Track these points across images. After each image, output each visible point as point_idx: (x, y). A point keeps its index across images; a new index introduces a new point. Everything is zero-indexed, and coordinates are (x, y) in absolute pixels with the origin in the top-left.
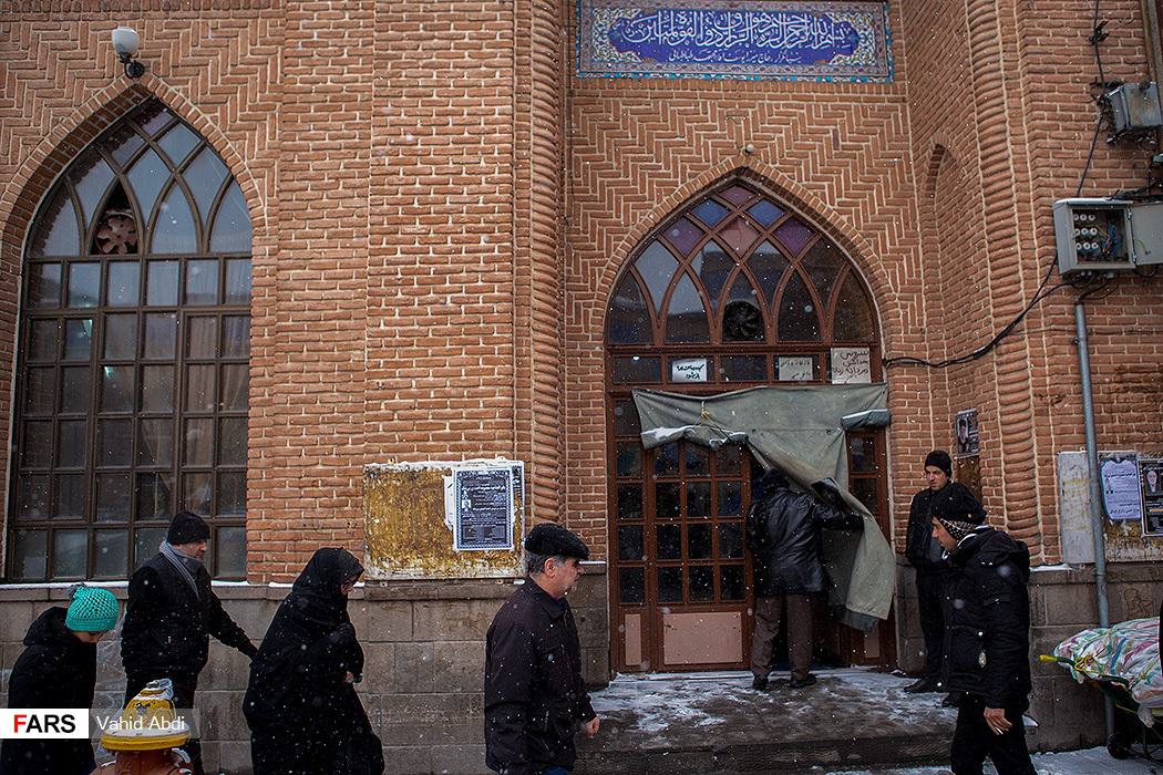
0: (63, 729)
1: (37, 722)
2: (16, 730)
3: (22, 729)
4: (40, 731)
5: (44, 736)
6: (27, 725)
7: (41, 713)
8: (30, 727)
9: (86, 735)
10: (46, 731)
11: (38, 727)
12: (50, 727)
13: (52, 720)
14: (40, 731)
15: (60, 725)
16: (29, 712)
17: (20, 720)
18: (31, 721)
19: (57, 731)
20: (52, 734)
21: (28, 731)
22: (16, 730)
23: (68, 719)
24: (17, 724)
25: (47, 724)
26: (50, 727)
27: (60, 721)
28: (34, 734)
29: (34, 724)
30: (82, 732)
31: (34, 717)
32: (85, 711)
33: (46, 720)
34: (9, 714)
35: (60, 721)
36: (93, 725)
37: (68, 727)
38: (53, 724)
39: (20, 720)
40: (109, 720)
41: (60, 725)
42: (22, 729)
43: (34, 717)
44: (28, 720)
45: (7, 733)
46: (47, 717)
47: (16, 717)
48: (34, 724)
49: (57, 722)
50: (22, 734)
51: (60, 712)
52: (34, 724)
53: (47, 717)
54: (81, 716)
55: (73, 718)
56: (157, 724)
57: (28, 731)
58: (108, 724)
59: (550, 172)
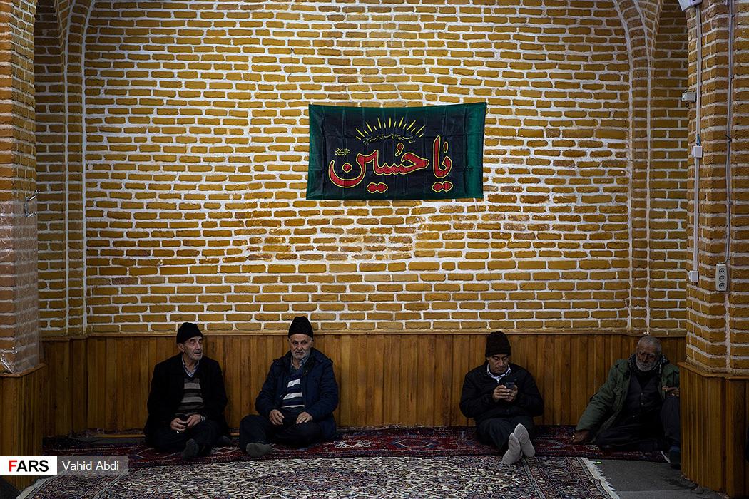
0: (41, 469)
1: (24, 465)
2: (10, 470)
3: (14, 469)
4: (26, 471)
5: (28, 474)
6: (17, 467)
7: (26, 459)
8: (19, 468)
10: (30, 470)
11: (25, 468)
12: (32, 468)
13: (33, 464)
14: (26, 471)
15: (39, 467)
16: (19, 459)
17: (13, 463)
18: (20, 465)
19: (37, 470)
20: (33, 473)
21: (18, 470)
22: (10, 470)
23: (44, 463)
24: (11, 466)
25: (30, 466)
26: (32, 468)
27: (39, 464)
28: (22, 473)
29: (22, 466)
30: (53, 471)
31: (22, 462)
32: (55, 458)
33: (30, 464)
34: (5, 460)
35: (39, 464)
36: (60, 468)
37: (44, 468)
38: (34, 466)
39: (13, 463)
40: (70, 463)
41: (39, 467)
42: (14, 469)
43: (22, 462)
44: (18, 464)
46: (30, 462)
47: (11, 462)
48: (22, 466)
49: (37, 465)
50: (14, 473)
51: (39, 459)
52: (22, 466)
53: (30, 462)
54: (52, 461)
55: (47, 462)
56: (101, 466)
57: (18, 470)
58: (70, 466)
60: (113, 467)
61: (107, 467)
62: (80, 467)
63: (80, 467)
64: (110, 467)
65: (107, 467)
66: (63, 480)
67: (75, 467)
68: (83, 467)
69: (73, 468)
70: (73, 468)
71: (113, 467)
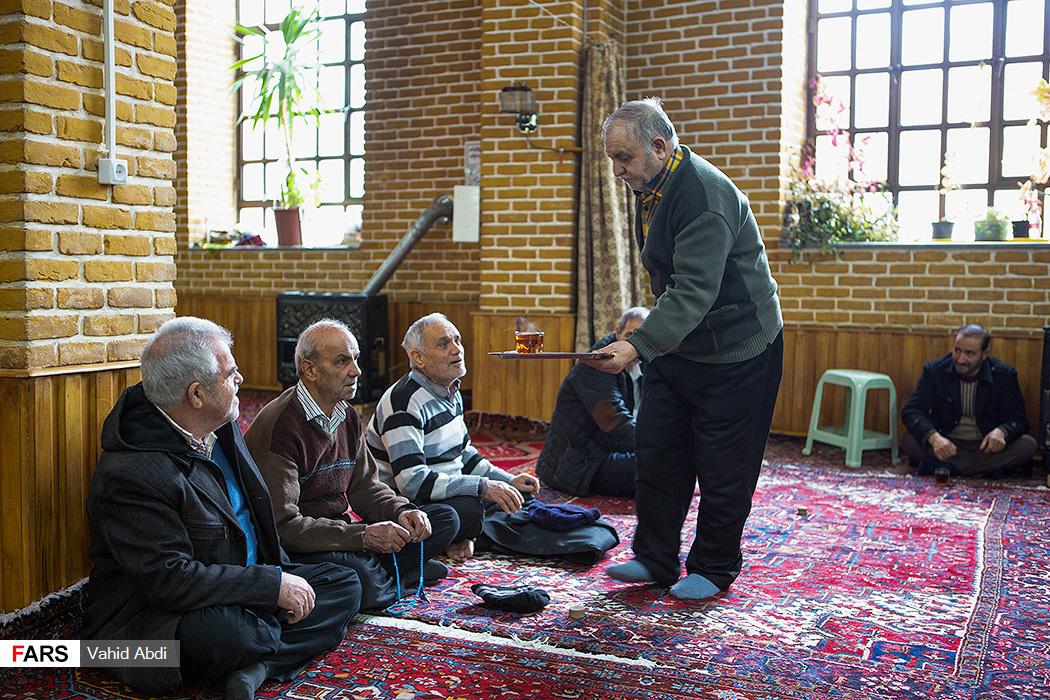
0: (57, 658)
1: (34, 652)
2: (15, 660)
3: (20, 658)
4: (36, 660)
5: (39, 664)
6: (24, 655)
7: (37, 644)
8: (27, 656)
9: (77, 664)
10: (42, 660)
11: (34, 656)
12: (45, 657)
13: (47, 650)
14: (36, 660)
15: (54, 655)
16: (26, 643)
17: (18, 650)
18: (28, 652)
19: (52, 660)
20: (47, 663)
21: (25, 660)
22: (15, 660)
23: (61, 650)
24: (15, 654)
25: (42, 654)
26: (45, 657)
27: (54, 651)
28: (31, 663)
29: (31, 654)
30: (74, 661)
31: (31, 648)
32: (77, 643)
33: (42, 650)
34: (7, 645)
35: (54, 651)
37: (62, 657)
38: (48, 654)
39: (18, 650)
40: (99, 650)
41: (54, 655)
42: (20, 658)
43: (31, 648)
44: (25, 650)
45: (8, 663)
46: (42, 647)
47: (15, 648)
48: (30, 654)
49: (51, 652)
50: (20, 663)
51: (54, 643)
52: (31, 654)
53: (42, 647)
54: (74, 647)
55: (65, 649)
56: (142, 654)
57: (25, 660)
58: (98, 654)
60: (158, 655)
61: (150, 655)
62: (112, 655)
63: (112, 655)
64: (154, 655)
65: (150, 655)
66: (90, 673)
67: (106, 655)
68: (117, 655)
69: (103, 656)
70: (103, 656)
71: (158, 655)
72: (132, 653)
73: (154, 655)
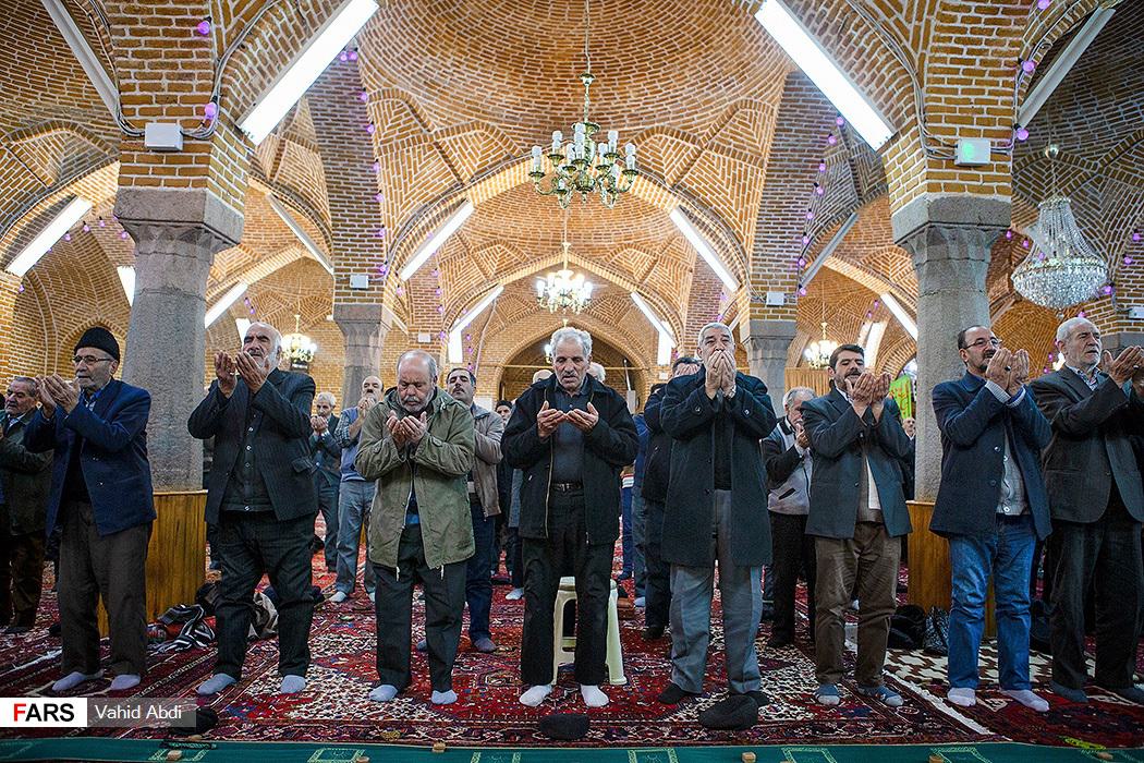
0: (62, 718)
1: (37, 711)
2: (16, 719)
3: (22, 717)
4: (40, 720)
5: (43, 724)
7: (40, 702)
8: (30, 715)
10: (46, 719)
11: (37, 715)
12: (49, 716)
13: (51, 709)
14: (40, 720)
15: (59, 713)
16: (29, 701)
17: (19, 709)
18: (31, 710)
19: (56, 719)
20: (51, 723)
21: (28, 719)
22: (16, 719)
23: (67, 708)
24: (16, 712)
25: (46, 713)
26: (49, 716)
27: (59, 710)
28: (34, 723)
29: (34, 713)
30: (81, 720)
31: (34, 706)
32: (84, 701)
33: (46, 709)
34: (8, 703)
35: (59, 710)
36: (91, 713)
37: (67, 716)
38: (52, 713)
39: (19, 709)
41: (59, 713)
42: (22, 717)
43: (34, 706)
44: (27, 709)
45: (9, 723)
46: (46, 706)
47: (16, 706)
48: (33, 712)
49: (56, 711)
50: (22, 723)
51: (59, 701)
52: (34, 713)
53: (46, 706)
54: (80, 705)
55: (71, 707)
56: (155, 713)
57: (28, 719)
59: (267, 552)
61: (163, 715)
62: (122, 713)
63: (122, 713)
64: (168, 714)
68: (128, 715)
69: (112, 715)
72: (144, 711)
73: (168, 714)
